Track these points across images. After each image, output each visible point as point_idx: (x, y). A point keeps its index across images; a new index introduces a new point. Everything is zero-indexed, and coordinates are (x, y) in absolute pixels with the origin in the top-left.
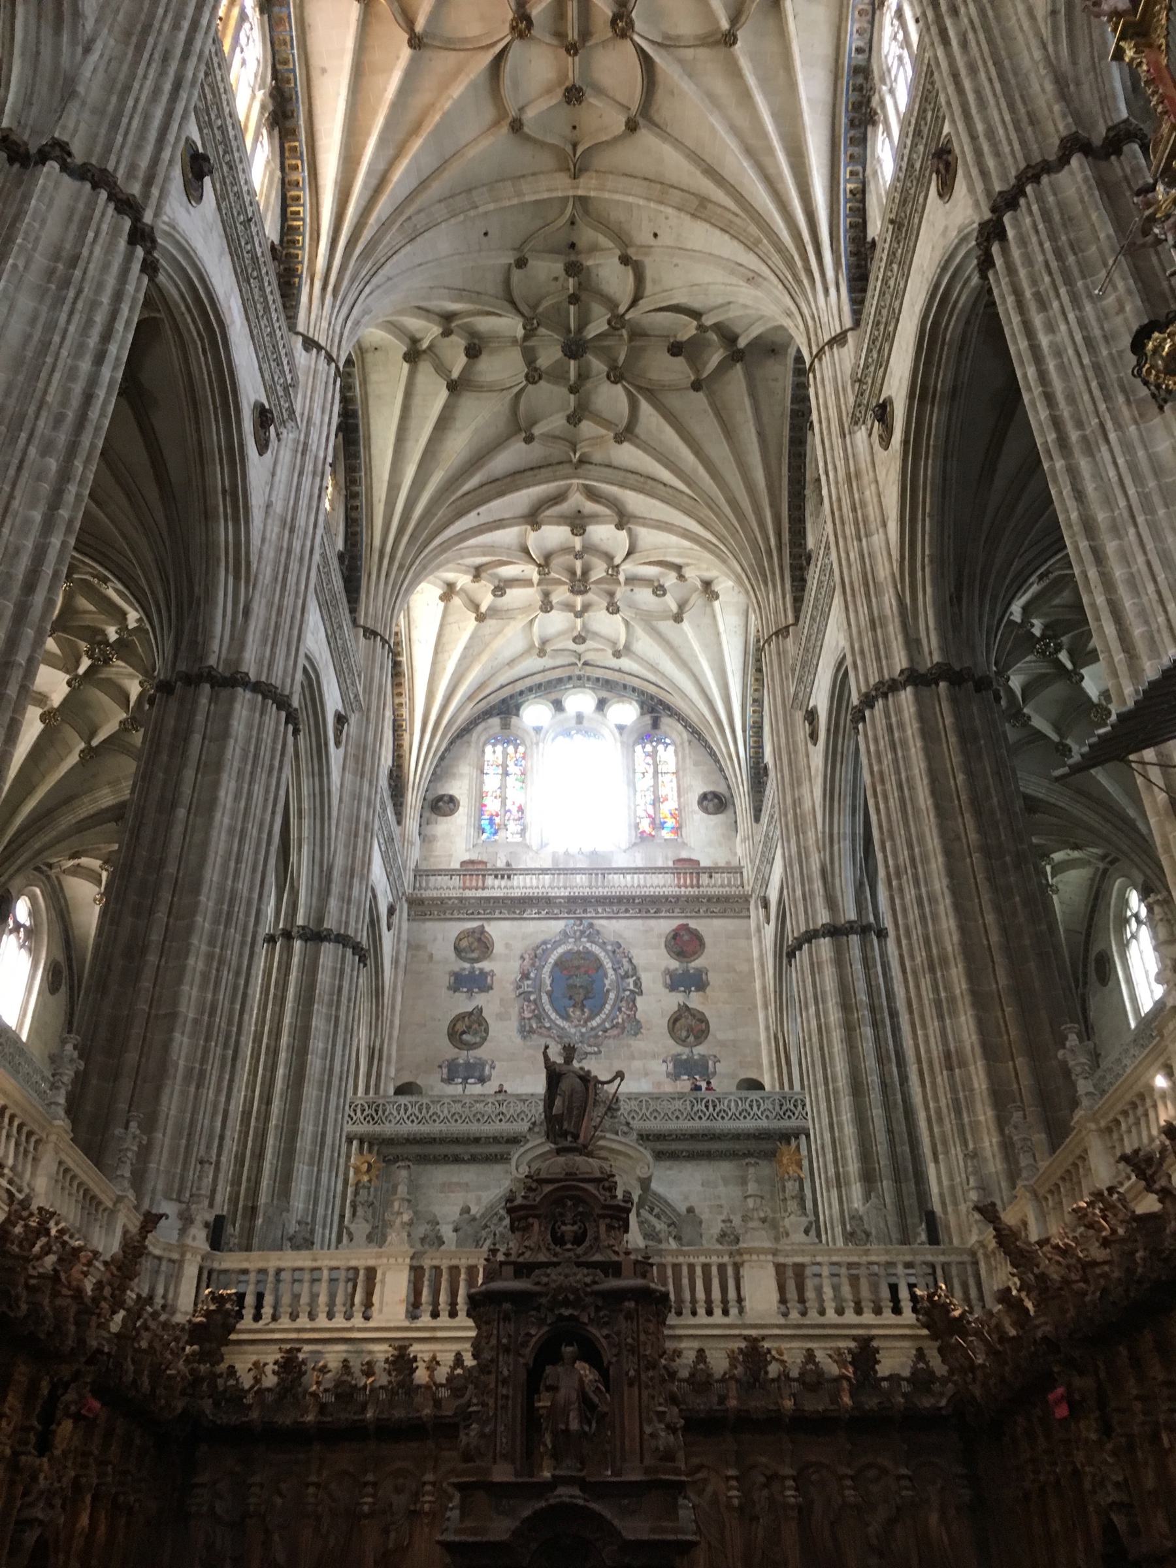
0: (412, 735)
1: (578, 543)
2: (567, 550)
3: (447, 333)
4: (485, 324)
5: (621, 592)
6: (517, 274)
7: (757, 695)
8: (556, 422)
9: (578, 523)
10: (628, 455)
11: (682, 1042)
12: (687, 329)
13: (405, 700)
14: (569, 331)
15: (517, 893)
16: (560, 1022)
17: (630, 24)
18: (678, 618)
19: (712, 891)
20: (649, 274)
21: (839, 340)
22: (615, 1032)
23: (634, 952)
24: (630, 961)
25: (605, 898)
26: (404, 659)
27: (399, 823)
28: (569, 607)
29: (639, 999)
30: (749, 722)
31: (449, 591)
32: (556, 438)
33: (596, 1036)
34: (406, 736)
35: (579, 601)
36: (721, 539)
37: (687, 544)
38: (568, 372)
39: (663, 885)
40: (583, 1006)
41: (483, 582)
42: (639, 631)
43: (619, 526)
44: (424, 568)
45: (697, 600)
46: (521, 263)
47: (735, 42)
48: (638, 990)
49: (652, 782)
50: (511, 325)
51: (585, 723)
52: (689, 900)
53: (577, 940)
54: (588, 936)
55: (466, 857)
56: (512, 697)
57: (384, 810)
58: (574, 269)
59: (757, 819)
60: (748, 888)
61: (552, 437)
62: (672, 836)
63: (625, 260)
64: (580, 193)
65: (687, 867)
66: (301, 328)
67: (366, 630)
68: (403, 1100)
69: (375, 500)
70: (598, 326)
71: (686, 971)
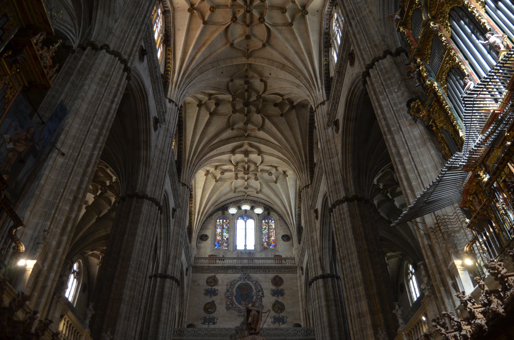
0: (195, 216)
1: (246, 159)
2: (243, 161)
3: (210, 99)
4: (221, 97)
5: (259, 174)
6: (230, 84)
7: (299, 205)
8: (241, 125)
9: (246, 153)
10: (262, 134)
11: (276, 312)
12: (279, 99)
13: (193, 205)
14: (245, 99)
15: (226, 265)
16: (238, 305)
17: (264, 20)
18: (276, 182)
19: (285, 265)
20: (268, 84)
21: (323, 103)
23: (262, 284)
24: (260, 287)
26: (193, 193)
28: (243, 178)
30: (297, 213)
31: (208, 173)
32: (241, 129)
34: (193, 216)
35: (246, 176)
36: (289, 159)
37: (279, 160)
38: (244, 110)
39: (270, 263)
41: (218, 170)
42: (264, 186)
43: (259, 155)
44: (200, 166)
45: (281, 177)
46: (232, 81)
47: (292, 25)
50: (228, 97)
51: (248, 213)
52: (279, 268)
53: (244, 280)
55: (210, 254)
57: (186, 238)
58: (247, 82)
59: (299, 243)
60: (297, 264)
61: (239, 129)
63: (262, 80)
64: (249, 62)
65: (278, 258)
66: (168, 97)
67: (182, 183)
68: (189, 329)
70: (254, 98)
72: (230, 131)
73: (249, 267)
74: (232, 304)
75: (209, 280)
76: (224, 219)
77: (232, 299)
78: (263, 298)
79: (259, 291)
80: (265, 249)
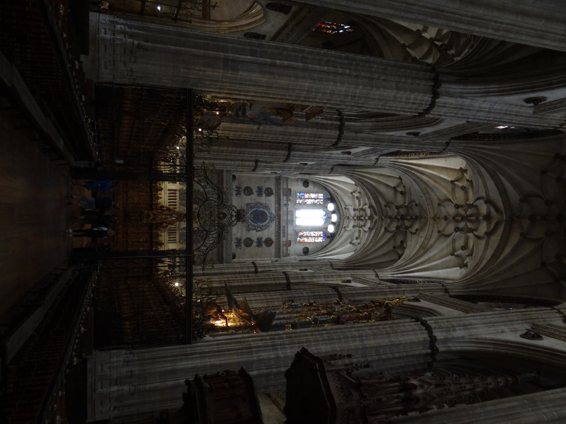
8: (390, 213)
9: (371, 218)
23: (267, 230)
24: (264, 229)
27: (300, 174)
29: (255, 231)
49: (312, 236)
51: (329, 219)
52: (280, 243)
54: (271, 219)
55: (292, 190)
60: (282, 258)
62: (298, 241)
65: (289, 244)
69: (368, 169)
71: (262, 242)
72: (384, 205)
74: (251, 208)
75: (269, 190)
77: (254, 207)
78: (255, 231)
79: (261, 228)
80: (296, 233)
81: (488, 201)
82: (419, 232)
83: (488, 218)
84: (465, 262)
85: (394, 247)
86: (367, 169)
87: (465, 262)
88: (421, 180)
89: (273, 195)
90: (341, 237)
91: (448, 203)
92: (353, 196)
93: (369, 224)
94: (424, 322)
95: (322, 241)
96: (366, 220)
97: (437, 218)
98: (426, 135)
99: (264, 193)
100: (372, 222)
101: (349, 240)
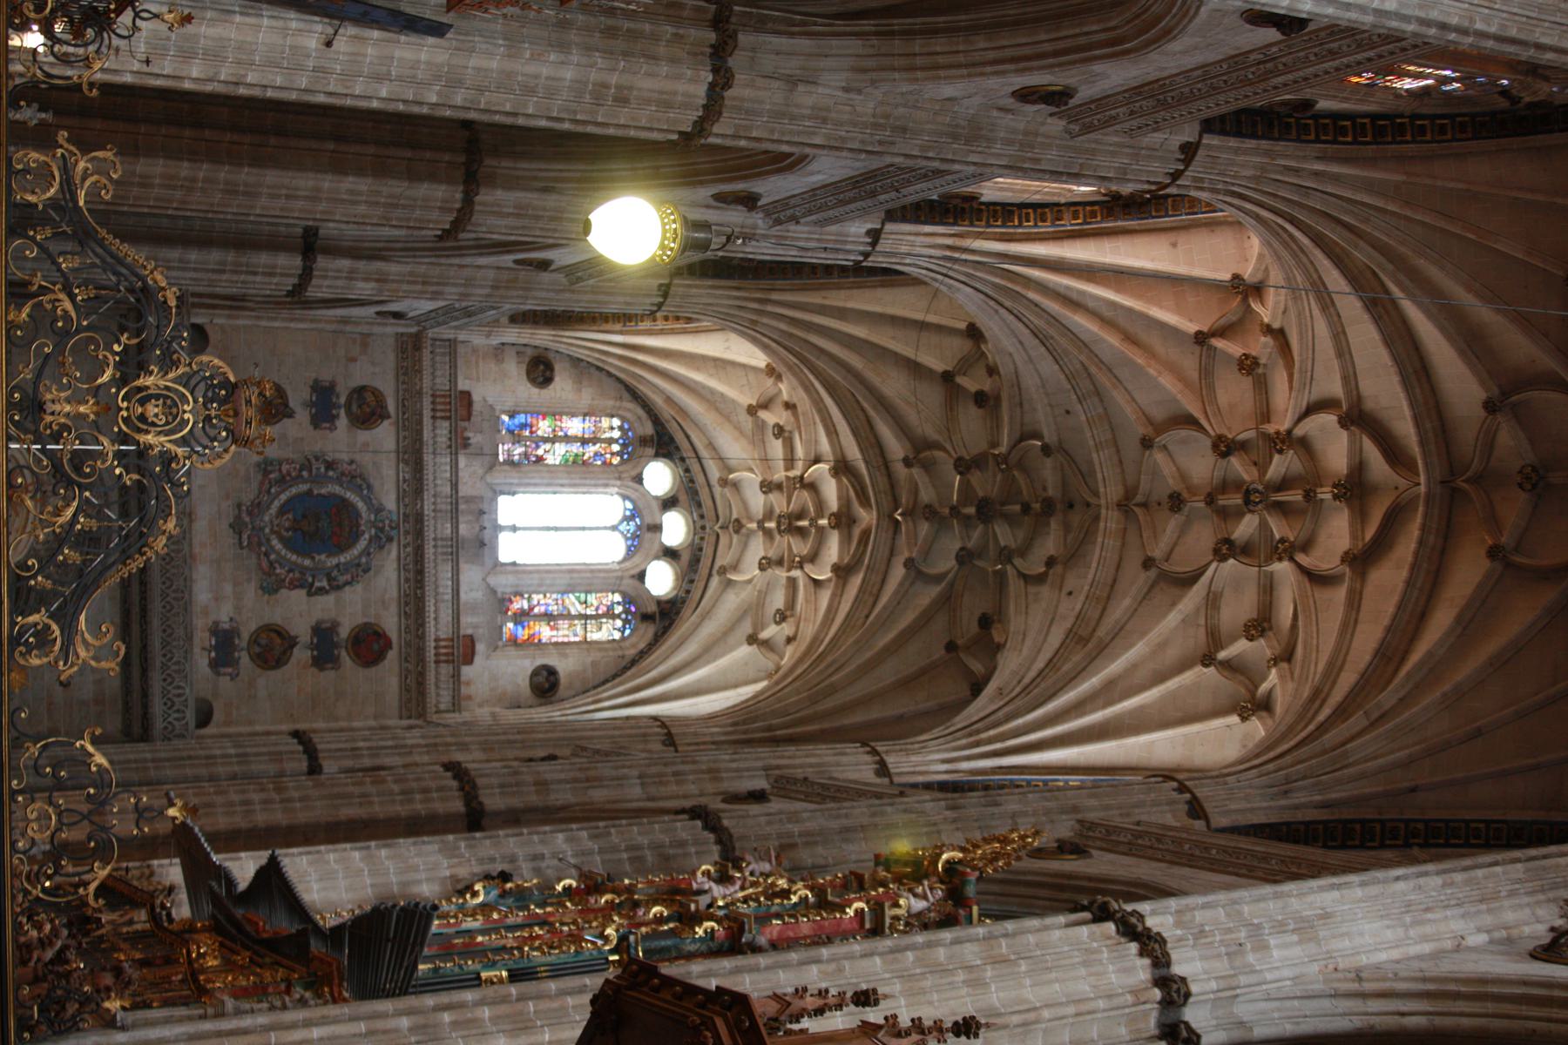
9: (843, 520)
15: (428, 458)
16: (276, 504)
22: (265, 564)
23: (359, 587)
24: (347, 583)
25: (422, 556)
29: (303, 592)
33: (260, 544)
35: (771, 525)
39: (438, 625)
40: (295, 530)
48: (313, 592)
52: (420, 651)
53: (373, 524)
54: (377, 536)
55: (476, 397)
56: (677, 448)
65: (463, 649)
73: (423, 540)
74: (283, 481)
75: (370, 398)
76: (624, 446)
77: (299, 479)
78: (303, 592)
79: (330, 579)
81: (1358, 418)
82: (1058, 569)
83: (1354, 489)
84: (1264, 687)
85: (951, 647)
86: (824, 293)
87: (1264, 687)
88: (1067, 330)
89: (386, 423)
90: (704, 617)
91: (1184, 433)
92: (761, 426)
93: (833, 550)
94: (1133, 920)
95: (617, 635)
96: (821, 530)
97: (1137, 505)
98: (1101, 102)
99: (342, 412)
100: (846, 540)
101: (746, 628)
